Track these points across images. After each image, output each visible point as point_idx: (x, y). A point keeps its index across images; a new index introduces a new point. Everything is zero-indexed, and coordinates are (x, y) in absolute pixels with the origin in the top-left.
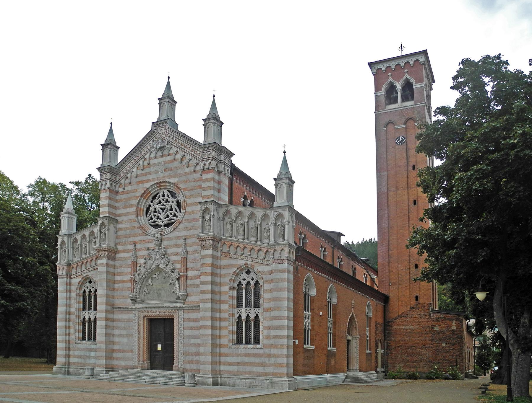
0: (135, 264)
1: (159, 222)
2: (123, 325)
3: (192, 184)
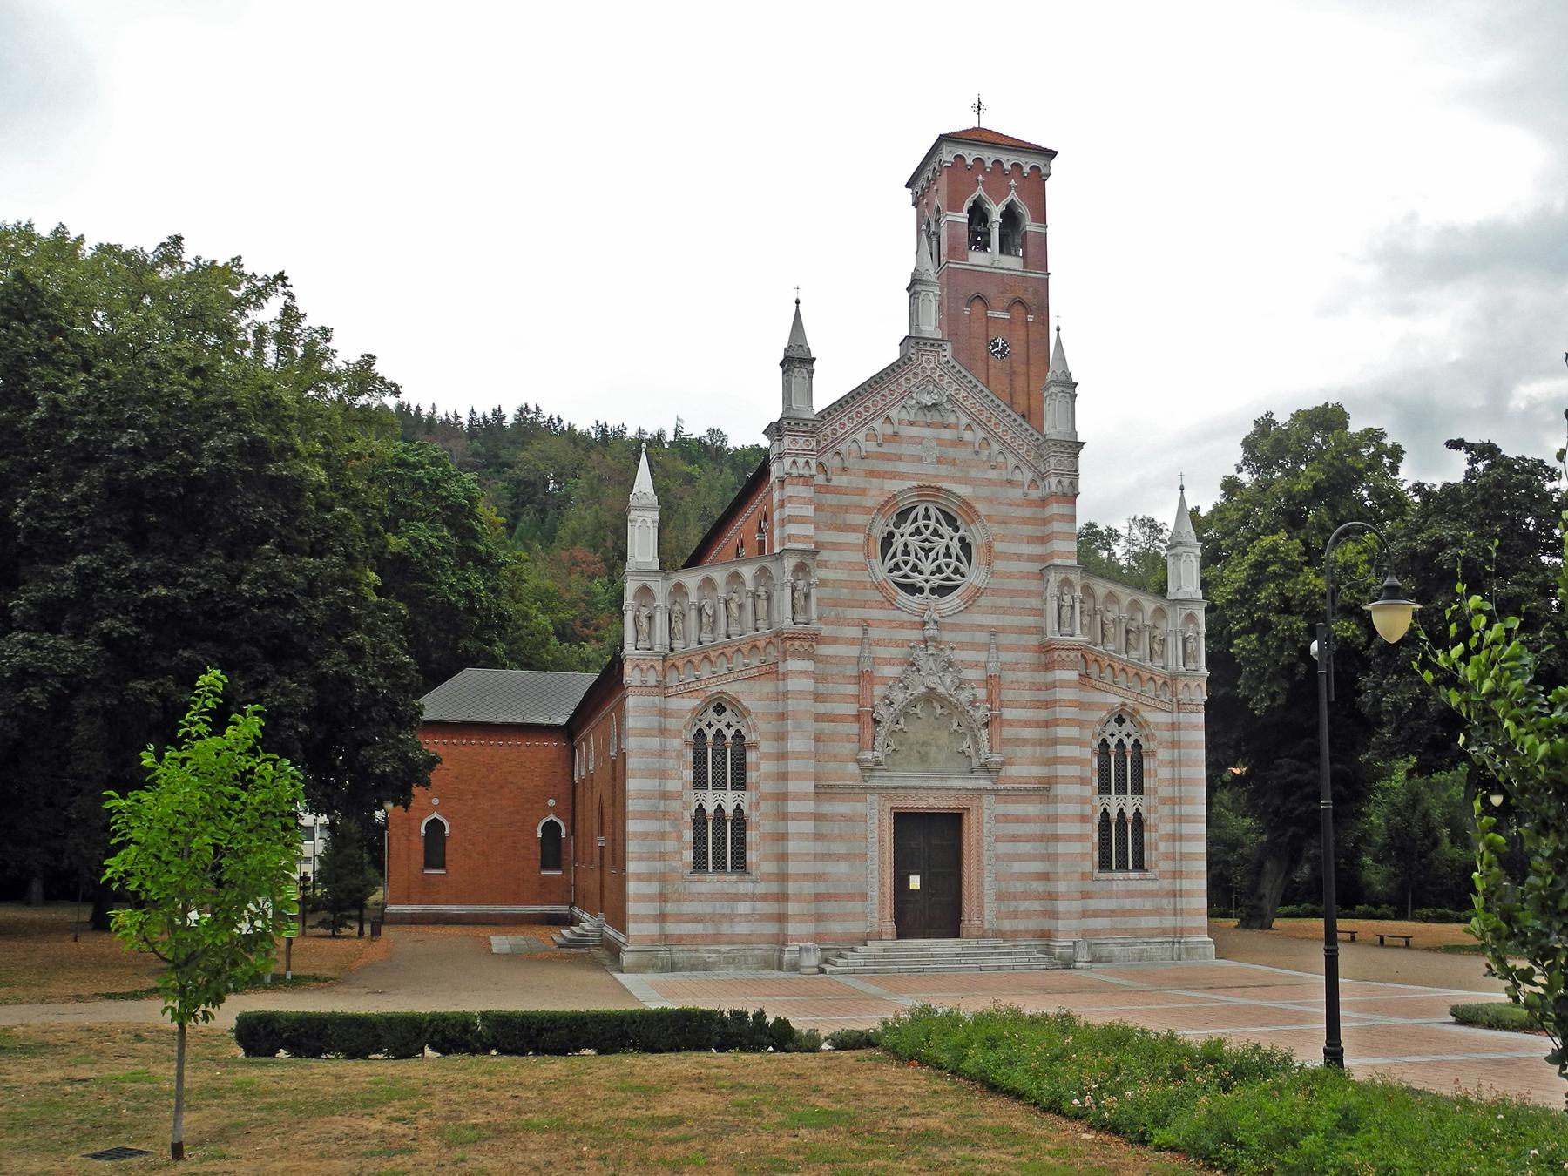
0: (864, 678)
1: (918, 579)
2: (836, 831)
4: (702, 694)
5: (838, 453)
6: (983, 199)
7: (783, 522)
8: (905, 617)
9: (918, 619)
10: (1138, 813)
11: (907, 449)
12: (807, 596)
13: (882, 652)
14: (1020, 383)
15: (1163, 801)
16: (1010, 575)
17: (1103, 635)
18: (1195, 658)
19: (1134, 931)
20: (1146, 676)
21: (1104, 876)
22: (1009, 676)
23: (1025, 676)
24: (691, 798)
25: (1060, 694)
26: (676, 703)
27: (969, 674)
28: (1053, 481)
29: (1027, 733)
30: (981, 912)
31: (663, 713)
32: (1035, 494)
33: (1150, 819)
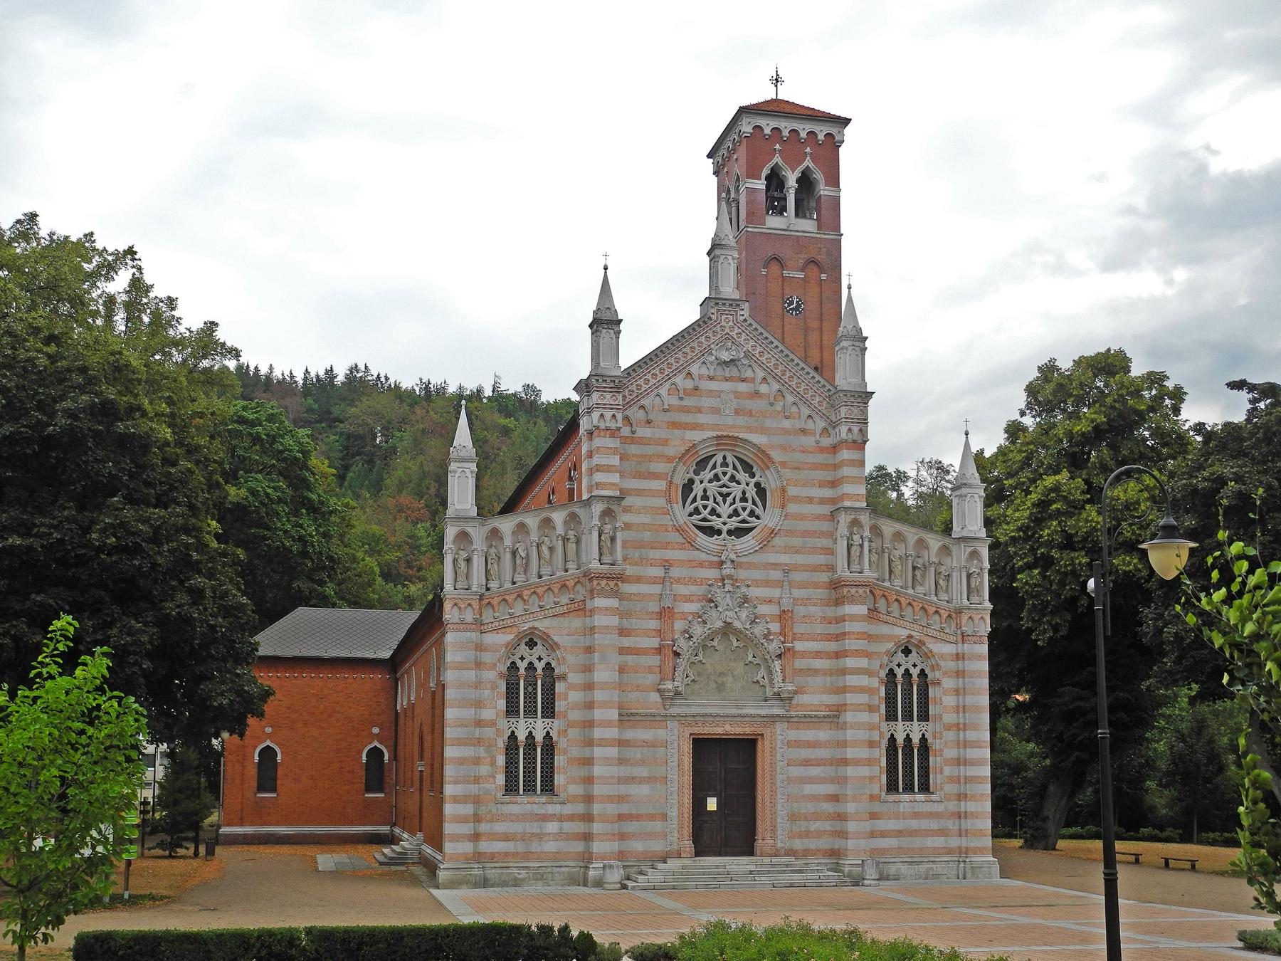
0: (666, 614)
1: (716, 522)
2: (639, 755)
3: (798, 456)
4: (515, 630)
5: (642, 407)
6: (780, 167)
7: (591, 471)
8: (703, 556)
9: (716, 559)
10: (923, 739)
11: (707, 402)
12: (613, 539)
13: (683, 590)
14: (814, 337)
15: (948, 727)
16: (801, 517)
17: (891, 572)
18: (979, 591)
19: (921, 850)
20: (931, 610)
21: (892, 798)
22: (801, 610)
23: (816, 611)
24: (504, 725)
25: (849, 627)
26: (490, 639)
27: (764, 609)
28: (844, 429)
29: (818, 664)
30: (774, 831)
31: (479, 647)
32: (826, 442)
33: (935, 744)
